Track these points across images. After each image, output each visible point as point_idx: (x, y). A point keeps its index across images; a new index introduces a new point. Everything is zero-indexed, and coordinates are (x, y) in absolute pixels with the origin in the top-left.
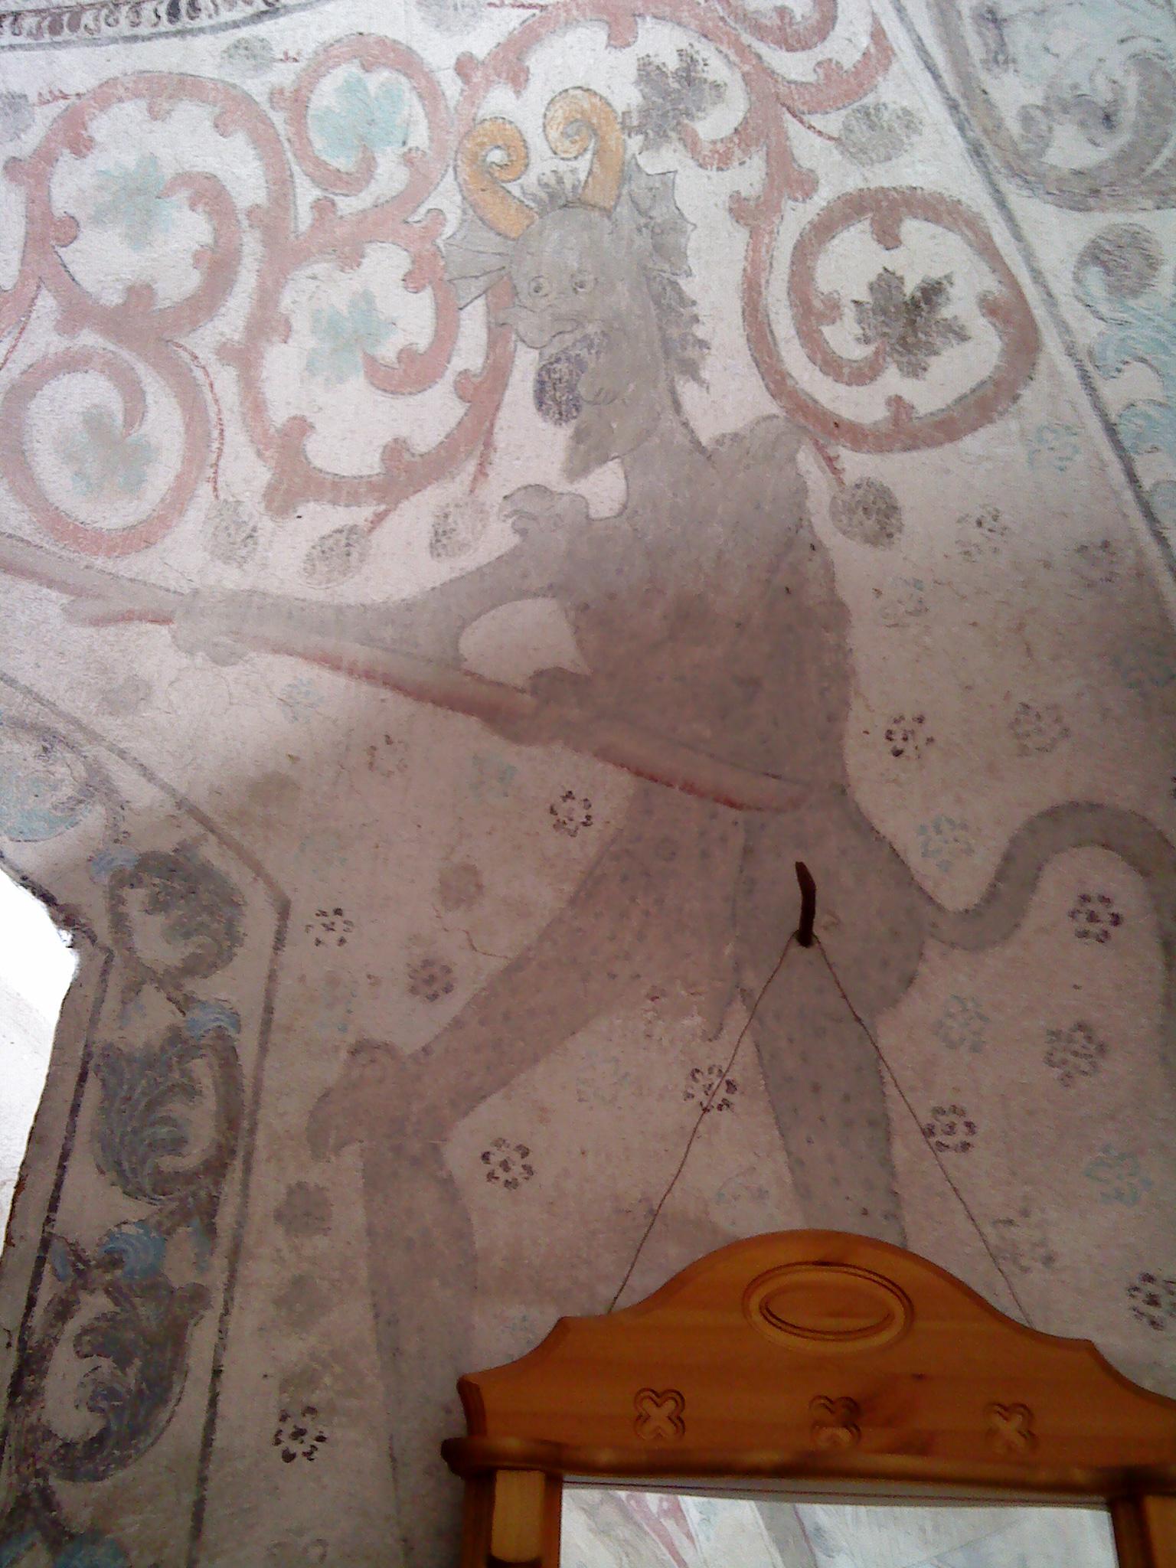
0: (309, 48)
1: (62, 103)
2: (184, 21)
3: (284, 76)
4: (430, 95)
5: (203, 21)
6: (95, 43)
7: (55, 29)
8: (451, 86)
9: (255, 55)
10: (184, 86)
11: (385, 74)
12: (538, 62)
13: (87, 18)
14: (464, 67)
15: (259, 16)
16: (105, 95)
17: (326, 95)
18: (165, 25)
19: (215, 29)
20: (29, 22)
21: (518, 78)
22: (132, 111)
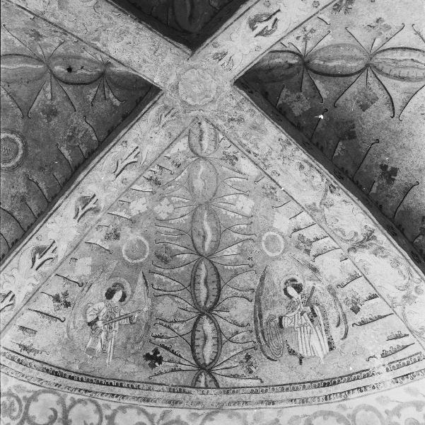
0: (354, 407)
1: (306, 417)
2: (328, 401)
3: (350, 411)
4: (380, 416)
5: (332, 401)
6: (311, 405)
7: (303, 403)
8: (385, 416)
9: (344, 408)
10: (330, 413)
11: (371, 412)
12: (402, 412)
13: (309, 400)
14: (387, 412)
15: (343, 400)
16: (315, 415)
17: (358, 416)
18: (325, 401)
19: (335, 402)
20: (298, 401)
21: (399, 415)
22: (320, 418)
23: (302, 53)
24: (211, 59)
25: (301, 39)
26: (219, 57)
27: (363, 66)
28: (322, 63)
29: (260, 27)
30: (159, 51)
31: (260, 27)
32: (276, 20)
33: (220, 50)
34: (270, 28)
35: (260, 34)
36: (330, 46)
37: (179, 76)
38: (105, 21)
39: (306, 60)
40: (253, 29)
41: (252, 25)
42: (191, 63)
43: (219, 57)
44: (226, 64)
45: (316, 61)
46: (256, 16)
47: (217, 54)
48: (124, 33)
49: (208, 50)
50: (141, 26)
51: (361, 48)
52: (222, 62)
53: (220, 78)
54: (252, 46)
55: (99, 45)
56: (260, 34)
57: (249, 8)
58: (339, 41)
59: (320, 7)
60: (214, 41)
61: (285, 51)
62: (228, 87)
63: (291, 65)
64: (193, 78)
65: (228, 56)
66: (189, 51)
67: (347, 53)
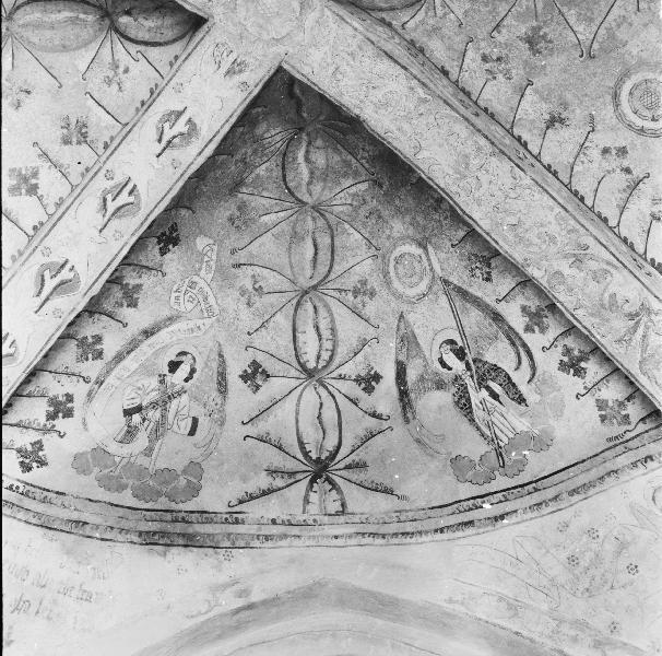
23: (115, 36)
24: (249, 60)
25: (121, 69)
26: (236, 68)
27: (15, 17)
28: (82, 16)
29: (181, 126)
30: (330, 72)
31: (181, 126)
32: (160, 141)
33: (238, 78)
34: (167, 125)
35: (179, 114)
36: (78, 48)
37: (301, 27)
38: (406, 126)
39: (107, 22)
40: (190, 120)
41: (192, 125)
42: (281, 49)
43: (236, 68)
44: (225, 54)
45: (90, 18)
46: (188, 143)
47: (240, 71)
48: (379, 106)
49: (256, 77)
50: (357, 111)
51: (30, 47)
52: (231, 59)
53: (231, 28)
54: (188, 90)
55: (421, 92)
56: (179, 114)
57: (200, 153)
58: (64, 58)
59: (103, 171)
60: (246, 94)
61: (146, 43)
62: (217, 13)
63: (128, 13)
64: (277, 21)
65: (224, 69)
66: (285, 66)
67: (48, 34)
